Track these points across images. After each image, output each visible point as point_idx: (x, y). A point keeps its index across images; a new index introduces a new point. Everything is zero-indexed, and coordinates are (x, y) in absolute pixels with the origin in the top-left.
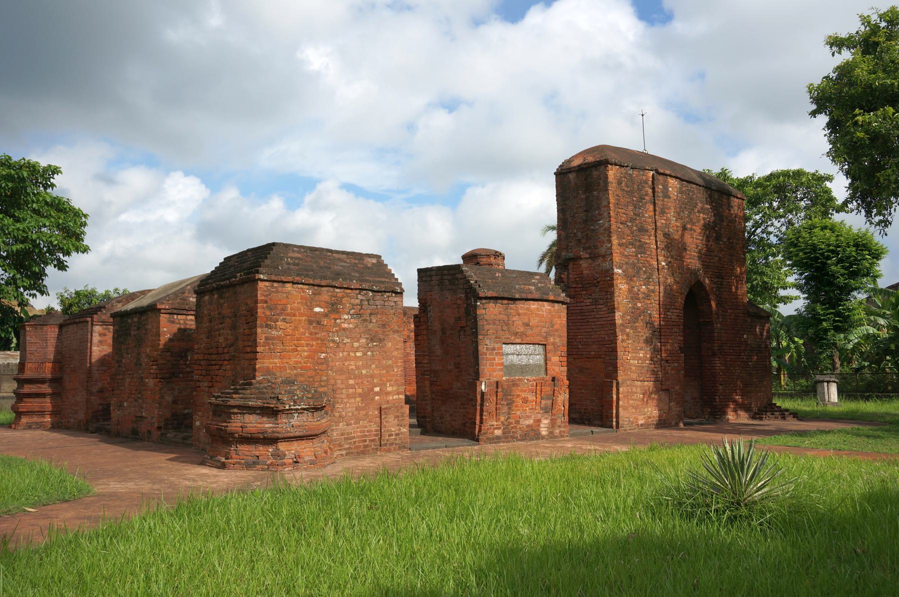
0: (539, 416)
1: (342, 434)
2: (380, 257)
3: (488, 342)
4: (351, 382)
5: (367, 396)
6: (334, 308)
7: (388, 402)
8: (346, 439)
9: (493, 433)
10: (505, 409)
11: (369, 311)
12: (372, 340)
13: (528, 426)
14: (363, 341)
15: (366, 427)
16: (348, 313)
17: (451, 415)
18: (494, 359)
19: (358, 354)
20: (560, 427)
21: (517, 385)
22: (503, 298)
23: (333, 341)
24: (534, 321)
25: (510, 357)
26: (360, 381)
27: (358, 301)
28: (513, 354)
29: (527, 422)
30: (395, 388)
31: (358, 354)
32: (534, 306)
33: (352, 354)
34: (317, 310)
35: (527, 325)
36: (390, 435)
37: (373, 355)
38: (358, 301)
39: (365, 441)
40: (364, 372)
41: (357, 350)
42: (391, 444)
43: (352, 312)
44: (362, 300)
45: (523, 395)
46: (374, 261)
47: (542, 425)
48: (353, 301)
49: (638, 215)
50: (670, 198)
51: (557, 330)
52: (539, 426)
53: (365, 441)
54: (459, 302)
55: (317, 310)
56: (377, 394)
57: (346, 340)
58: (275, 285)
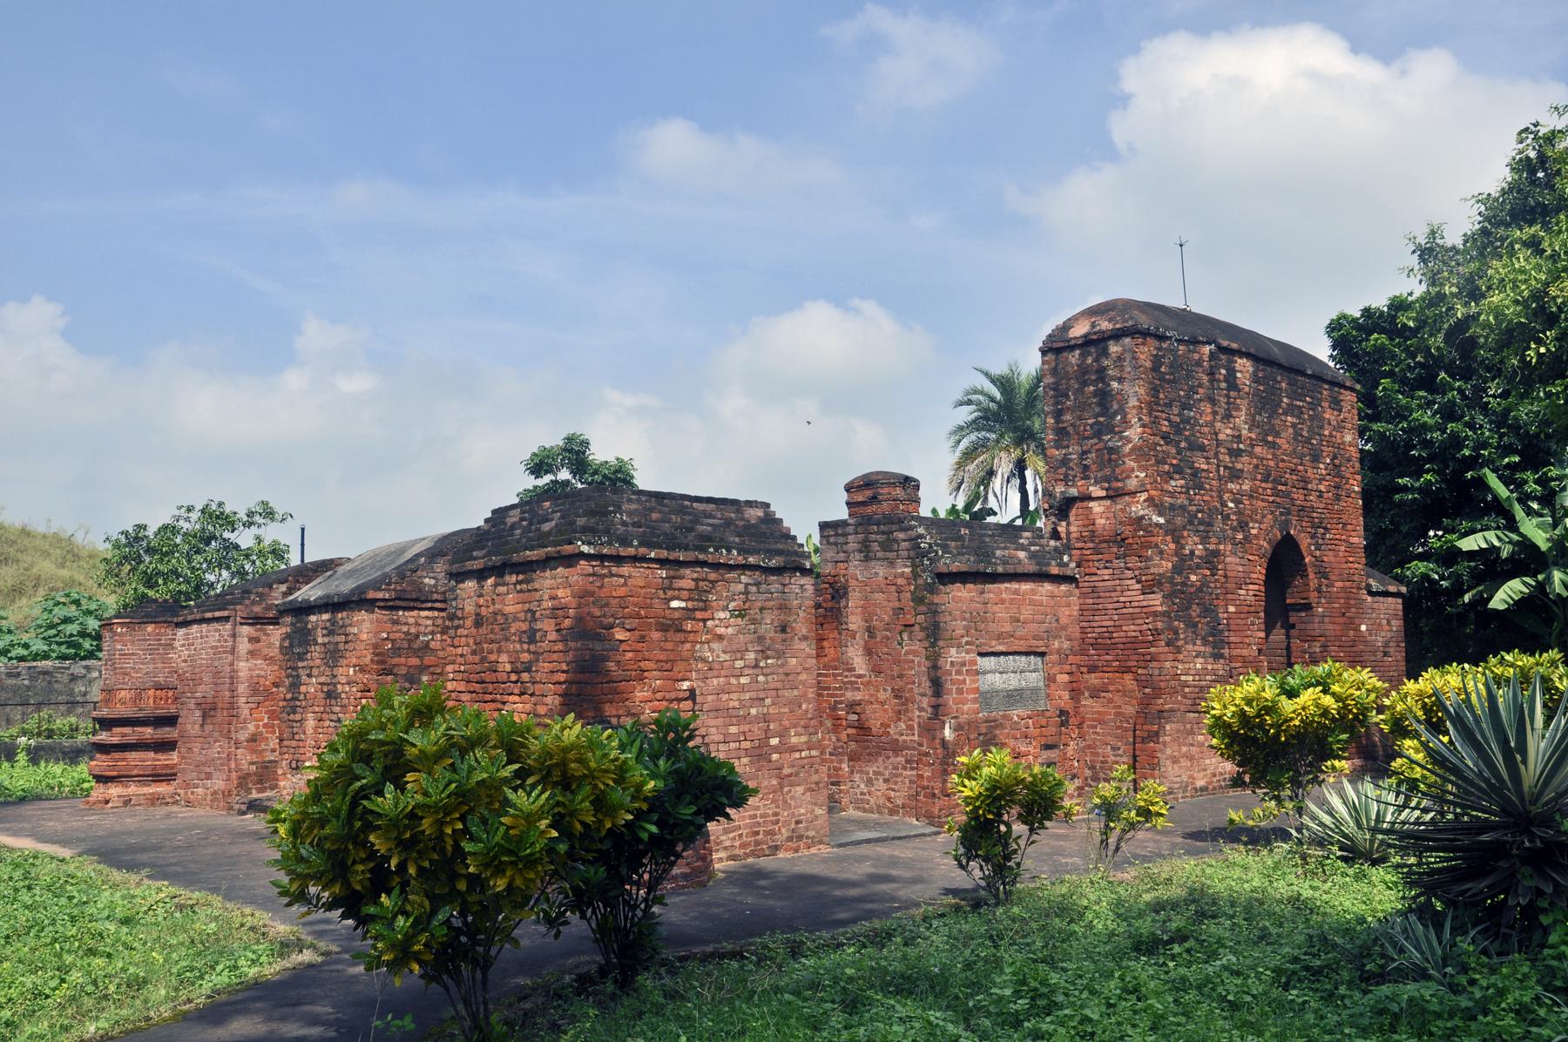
2: (768, 505)
4: (733, 729)
15: (757, 808)
16: (725, 608)
17: (886, 781)
19: (743, 680)
23: (704, 660)
24: (1026, 613)
26: (746, 728)
30: (804, 739)
31: (743, 680)
32: (1026, 587)
33: (733, 681)
34: (675, 604)
36: (798, 822)
38: (741, 587)
39: (757, 833)
40: (753, 711)
43: (732, 605)
44: (747, 585)
46: (760, 513)
49: (1187, 421)
51: (1064, 628)
53: (757, 833)
54: (900, 581)
55: (675, 604)
56: (776, 749)
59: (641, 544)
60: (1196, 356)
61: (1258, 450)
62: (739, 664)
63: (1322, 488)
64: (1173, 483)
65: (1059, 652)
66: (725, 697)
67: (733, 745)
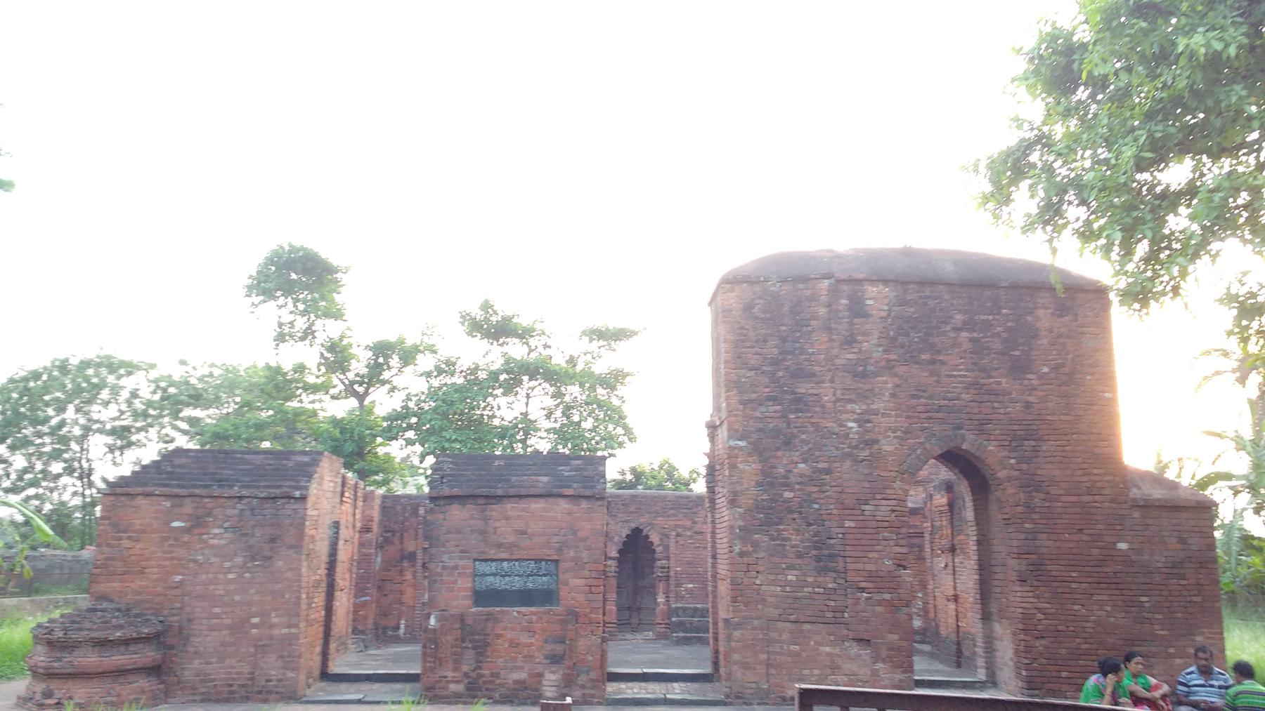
0: (540, 669)
1: (198, 675)
3: (445, 557)
4: (217, 610)
5: (239, 628)
6: (198, 523)
7: (271, 637)
8: (201, 681)
9: (445, 688)
10: (470, 654)
11: (252, 523)
12: (253, 558)
13: (516, 682)
14: (239, 560)
16: (221, 527)
18: (455, 582)
19: (230, 576)
20: (583, 687)
21: (497, 620)
22: (475, 497)
23: (195, 561)
25: (490, 579)
27: (236, 511)
28: (494, 575)
29: (516, 676)
30: (284, 619)
31: (230, 576)
32: (537, 506)
33: (221, 576)
34: (176, 524)
35: (524, 533)
36: (268, 681)
37: (252, 578)
39: (231, 686)
41: (229, 571)
42: (270, 692)
43: (226, 525)
45: (509, 635)
47: (545, 683)
48: (229, 512)
50: (866, 315)
51: (585, 539)
52: (540, 682)
55: (176, 524)
56: (254, 626)
57: (213, 560)
58: (122, 498)
59: (155, 485)
60: (808, 293)
61: (902, 370)
62: (227, 564)
63: (1031, 399)
64: (763, 409)
65: (575, 559)
66: (212, 587)
67: (215, 621)
